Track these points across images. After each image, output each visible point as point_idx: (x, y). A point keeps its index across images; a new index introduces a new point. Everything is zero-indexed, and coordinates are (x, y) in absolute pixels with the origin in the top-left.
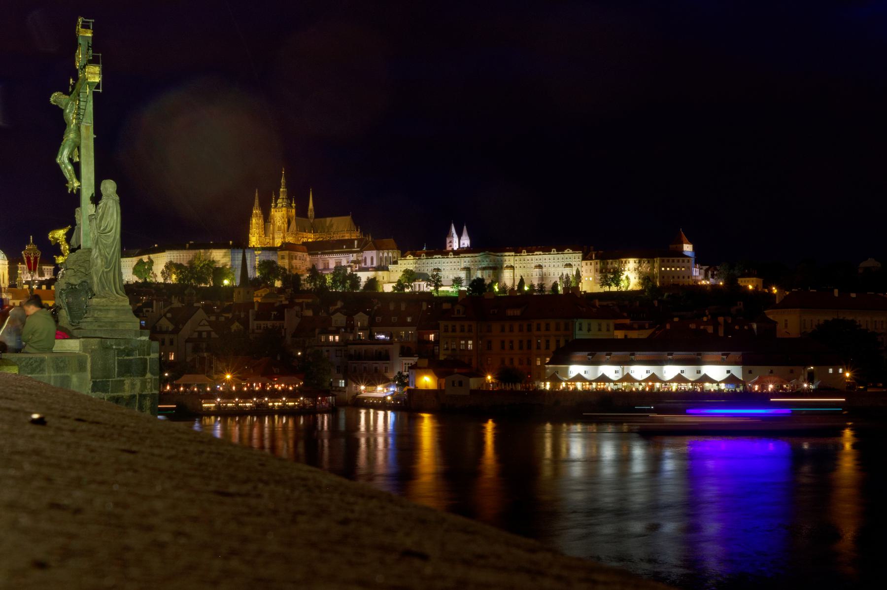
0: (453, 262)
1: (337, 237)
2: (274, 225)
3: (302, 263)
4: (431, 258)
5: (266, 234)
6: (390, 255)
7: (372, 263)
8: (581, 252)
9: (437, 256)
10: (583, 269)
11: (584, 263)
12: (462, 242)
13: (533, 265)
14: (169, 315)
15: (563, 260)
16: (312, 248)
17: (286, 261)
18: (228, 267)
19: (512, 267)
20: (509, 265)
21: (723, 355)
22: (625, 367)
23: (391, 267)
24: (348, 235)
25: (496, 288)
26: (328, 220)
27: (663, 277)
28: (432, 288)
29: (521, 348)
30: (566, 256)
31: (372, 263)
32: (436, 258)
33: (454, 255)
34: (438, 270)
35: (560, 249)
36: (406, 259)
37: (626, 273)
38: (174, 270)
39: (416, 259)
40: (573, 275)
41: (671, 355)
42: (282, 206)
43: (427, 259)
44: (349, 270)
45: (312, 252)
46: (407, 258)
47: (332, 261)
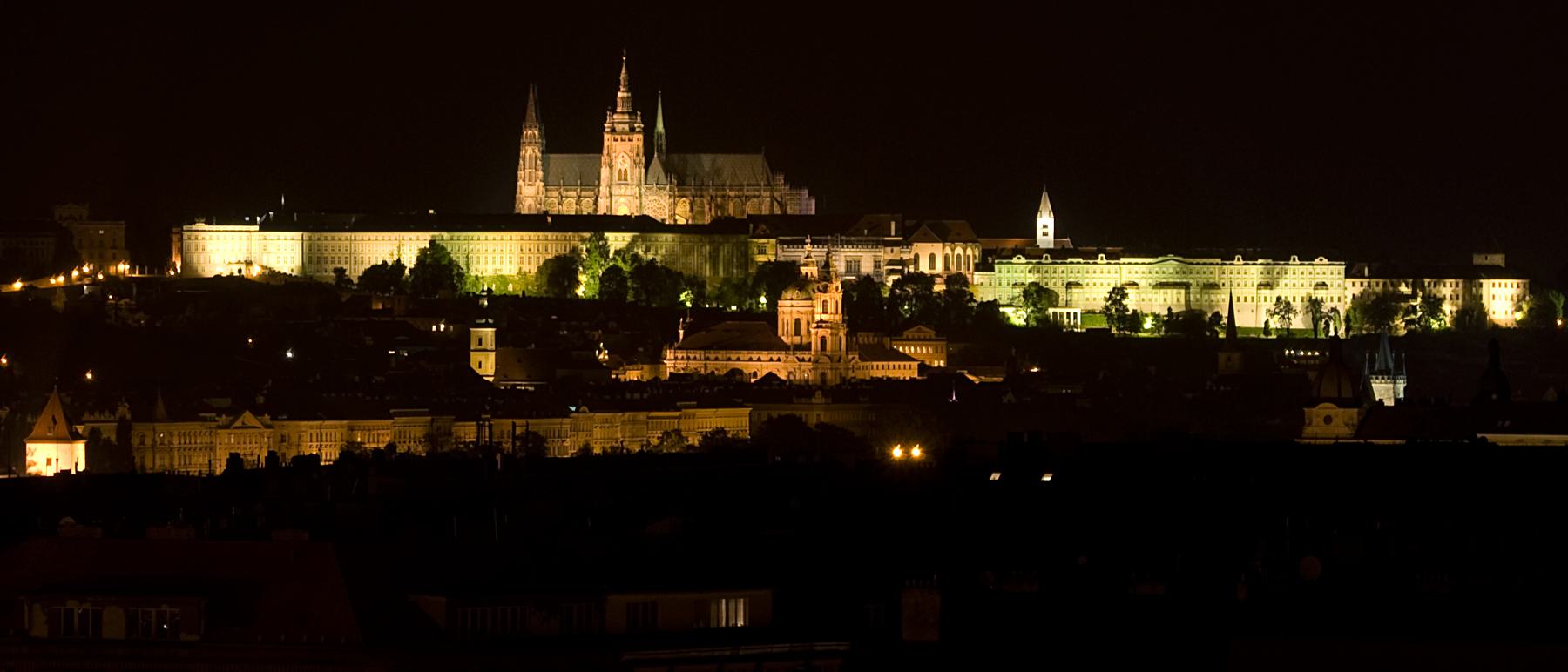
0: (1105, 271)
2: (611, 167)
4: (1062, 263)
6: (969, 252)
7: (932, 266)
8: (1343, 263)
9: (1075, 260)
11: (1349, 281)
15: (1312, 276)
20: (1211, 281)
24: (768, 193)
26: (706, 160)
27: (1494, 313)
30: (1318, 269)
31: (932, 266)
32: (1071, 263)
33: (1107, 258)
34: (1078, 284)
35: (1307, 256)
36: (1012, 263)
39: (1031, 263)
42: (632, 130)
43: (1053, 263)
45: (781, 238)
46: (1012, 261)
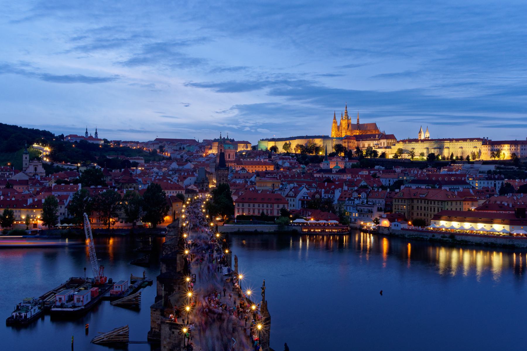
1: (369, 133)
3: (353, 145)
5: (338, 130)
6: (392, 141)
7: (384, 145)
9: (413, 142)
10: (482, 149)
12: (426, 135)
13: (458, 147)
14: (293, 190)
16: (358, 138)
17: (346, 144)
18: (322, 146)
19: (448, 148)
21: (502, 220)
22: (462, 223)
23: (392, 147)
25: (440, 158)
27: (522, 154)
28: (411, 157)
29: (425, 209)
31: (384, 145)
37: (503, 152)
38: (299, 148)
40: (477, 152)
41: (481, 219)
44: (373, 148)
47: (366, 144)
